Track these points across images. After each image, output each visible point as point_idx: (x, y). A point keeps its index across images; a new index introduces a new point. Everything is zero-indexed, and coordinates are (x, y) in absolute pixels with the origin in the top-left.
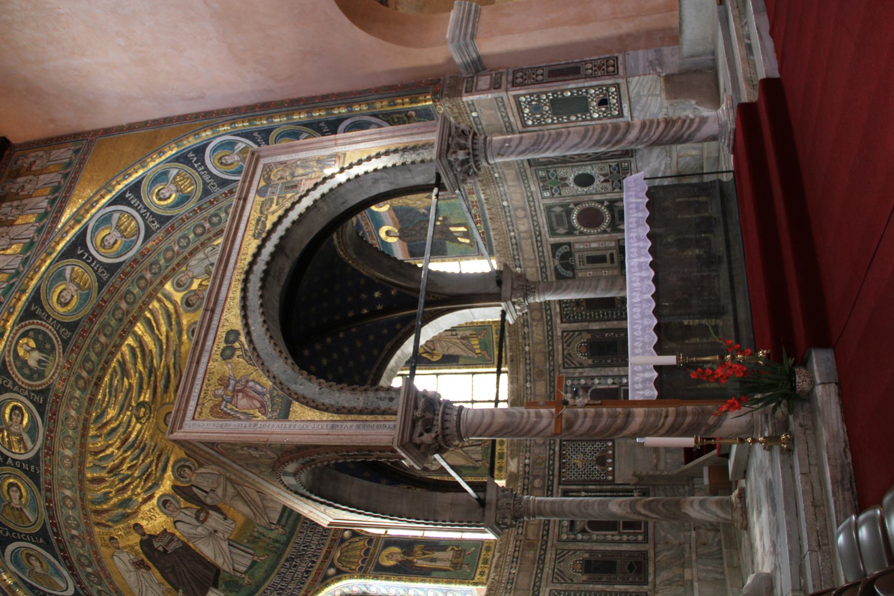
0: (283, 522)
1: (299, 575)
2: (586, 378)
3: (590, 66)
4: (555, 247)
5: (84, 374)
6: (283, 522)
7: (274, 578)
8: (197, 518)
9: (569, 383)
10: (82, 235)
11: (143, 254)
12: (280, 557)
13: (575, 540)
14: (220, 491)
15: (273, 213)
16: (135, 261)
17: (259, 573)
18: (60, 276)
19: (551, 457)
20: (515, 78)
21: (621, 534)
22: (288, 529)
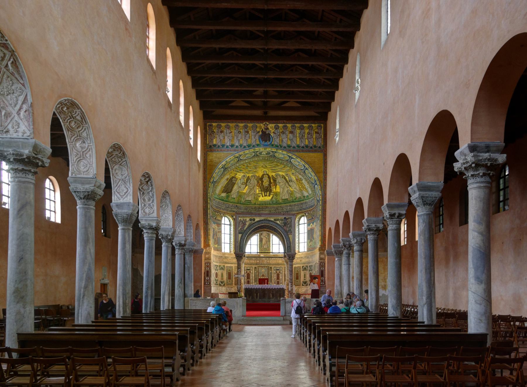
0: (246, 201)
1: (233, 210)
2: (282, 272)
3: (323, 279)
4: (307, 266)
5: (266, 159)
6: (246, 201)
7: (231, 204)
8: (243, 183)
9: (281, 268)
10: (294, 159)
11: (297, 167)
12: (237, 203)
13: (244, 270)
14: (251, 185)
15: (280, 222)
16: (295, 166)
17: (232, 201)
18: (284, 155)
19: (264, 264)
20: (322, 263)
21: (246, 280)
22: (244, 203)
